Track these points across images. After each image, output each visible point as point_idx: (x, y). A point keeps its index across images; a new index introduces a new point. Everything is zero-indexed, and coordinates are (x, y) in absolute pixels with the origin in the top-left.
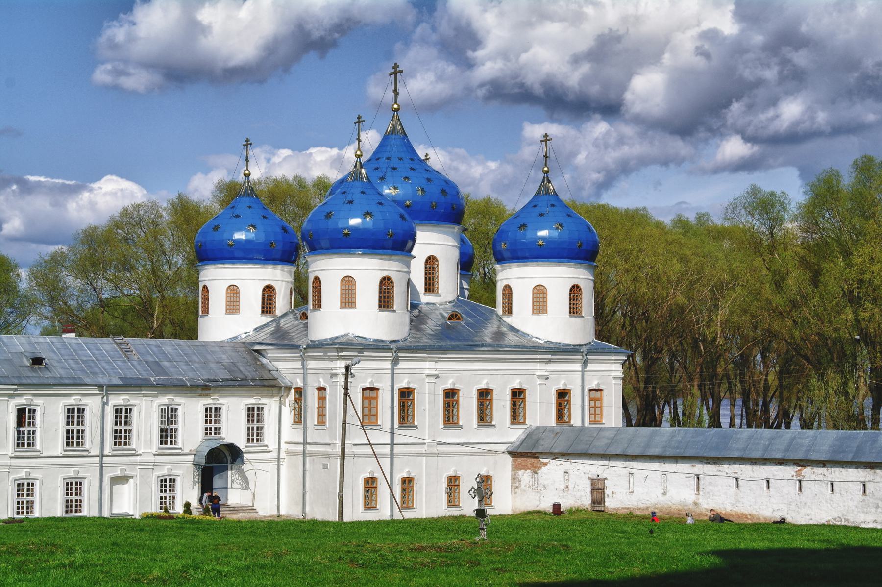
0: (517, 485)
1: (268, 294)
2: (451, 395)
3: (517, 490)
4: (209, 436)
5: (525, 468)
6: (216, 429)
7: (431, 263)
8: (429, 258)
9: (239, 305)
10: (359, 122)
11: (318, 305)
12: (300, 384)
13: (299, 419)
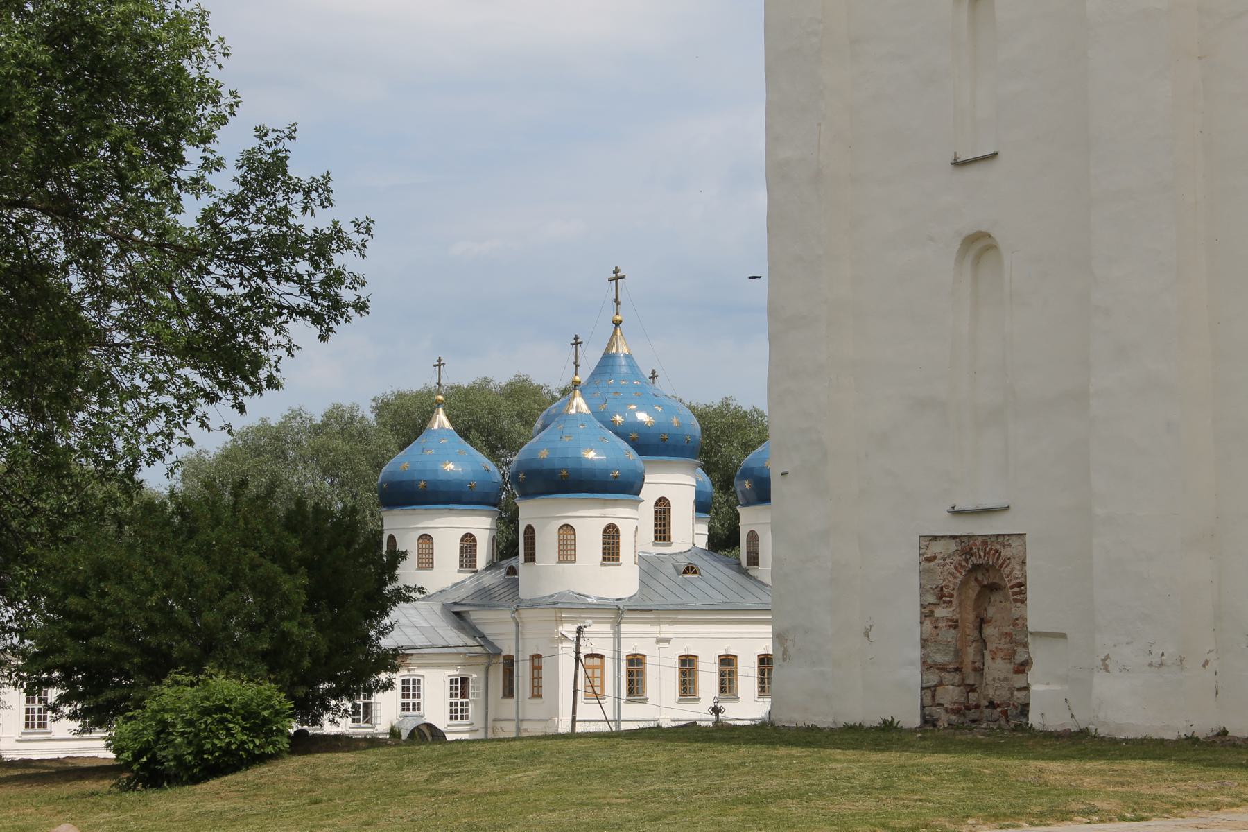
2: (688, 663)
4: (406, 713)
6: (414, 704)
7: (663, 509)
8: (660, 500)
10: (576, 344)
11: (531, 557)
12: (513, 653)
13: (509, 692)
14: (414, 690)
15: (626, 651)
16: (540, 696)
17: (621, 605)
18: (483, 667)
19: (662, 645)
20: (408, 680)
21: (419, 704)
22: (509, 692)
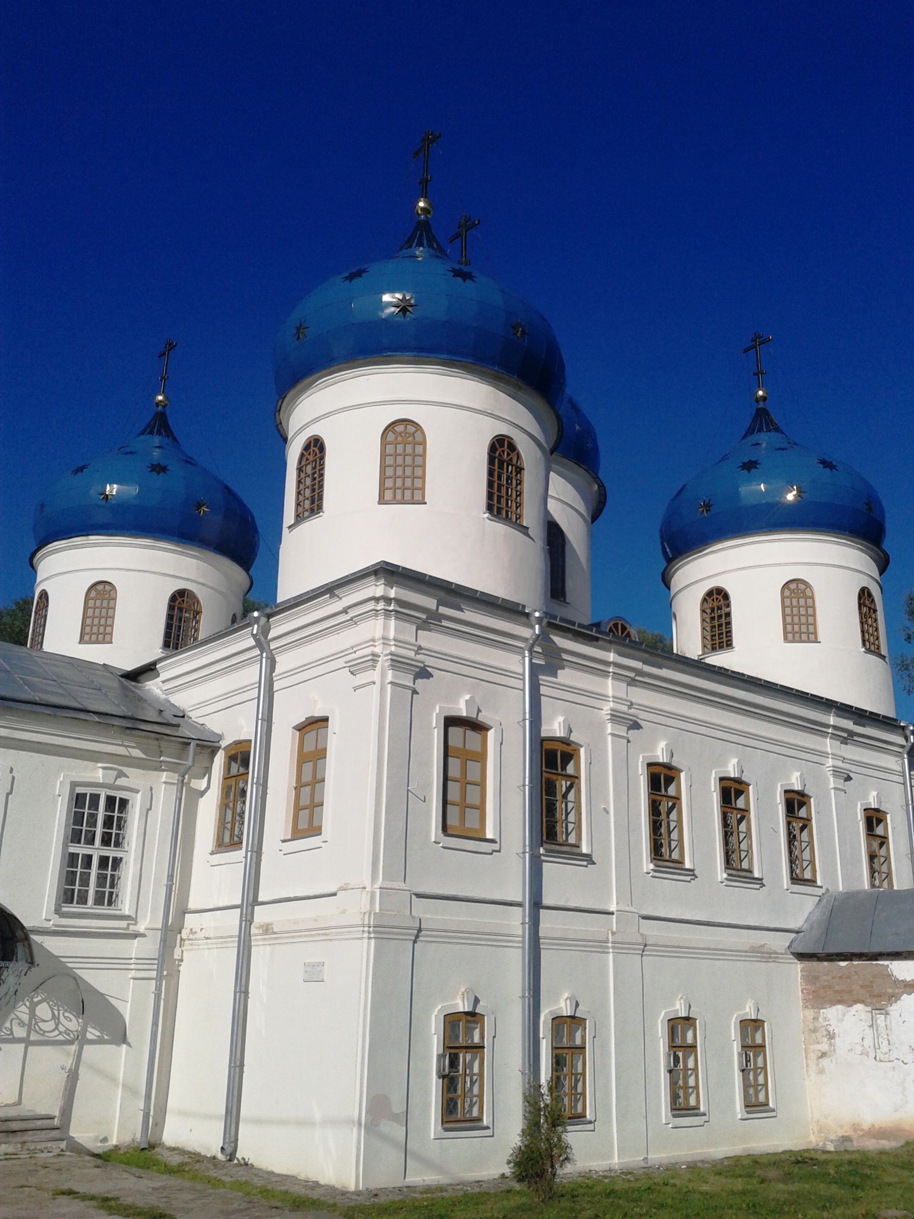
0: (824, 1047)
3: (824, 1062)
5: (846, 998)
9: (112, 626)
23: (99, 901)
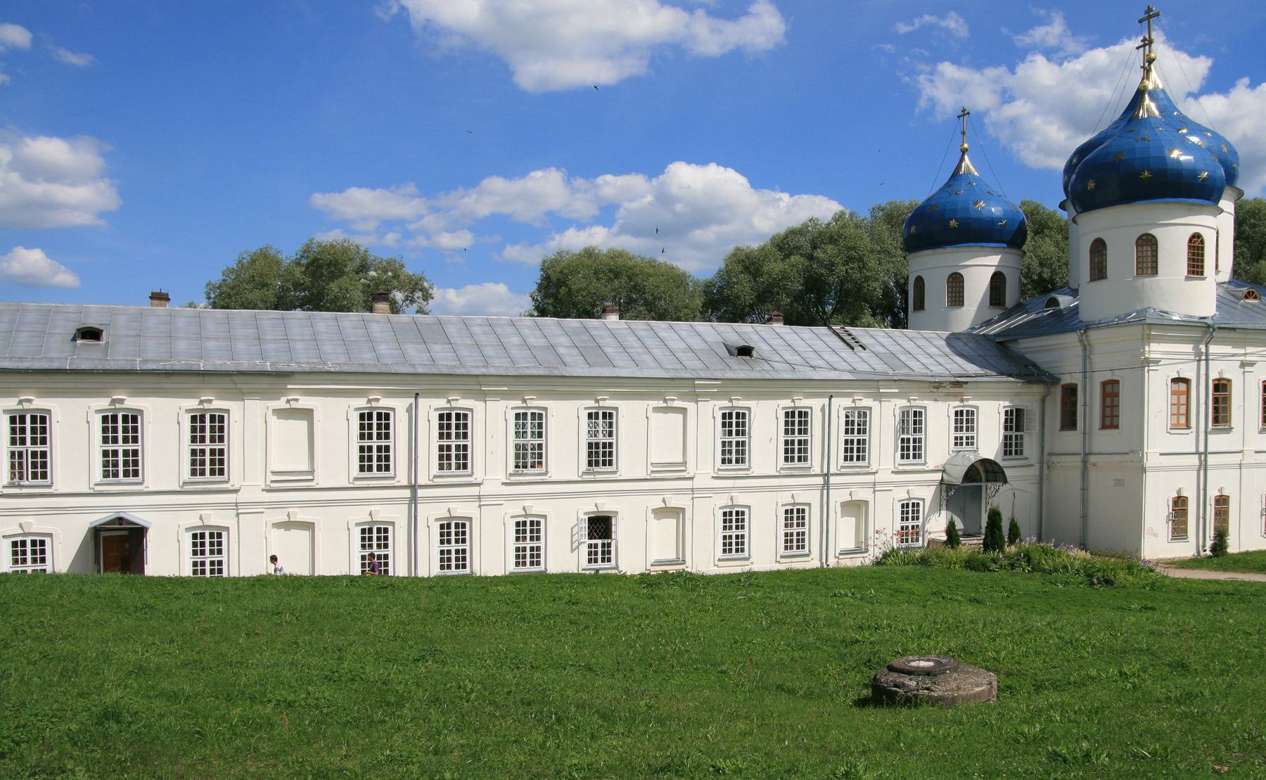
1: (997, 281)
4: (959, 448)
6: (967, 438)
12: (1076, 379)
13: (1069, 422)
14: (967, 422)
15: (1214, 375)
16: (1117, 427)
17: (1209, 322)
18: (1038, 398)
19: (1247, 369)
20: (962, 412)
21: (972, 438)
22: (1069, 422)
23: (1016, 453)
